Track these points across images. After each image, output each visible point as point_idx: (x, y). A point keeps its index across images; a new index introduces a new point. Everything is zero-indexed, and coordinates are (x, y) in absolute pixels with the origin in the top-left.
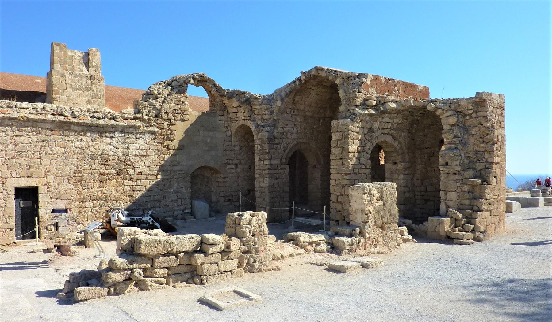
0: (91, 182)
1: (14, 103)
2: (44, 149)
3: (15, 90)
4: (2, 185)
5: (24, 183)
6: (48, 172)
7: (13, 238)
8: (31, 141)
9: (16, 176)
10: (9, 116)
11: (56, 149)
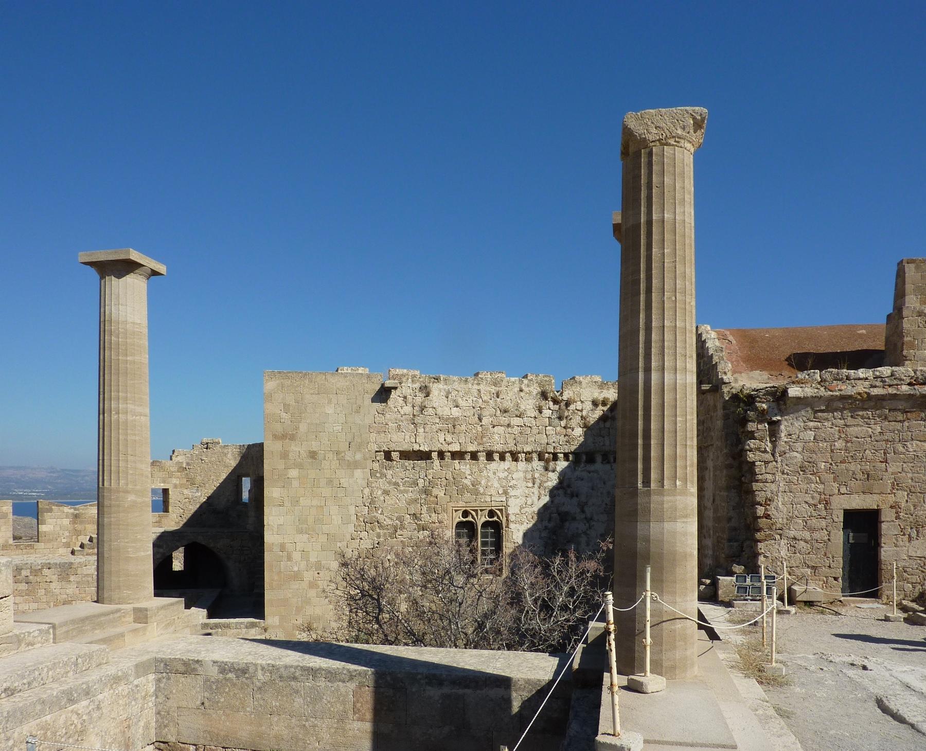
1: (845, 372)
2: (892, 446)
3: (831, 351)
4: (825, 506)
5: (858, 502)
6: (897, 484)
7: (838, 594)
8: (871, 433)
9: (846, 492)
10: (841, 395)
11: (912, 444)
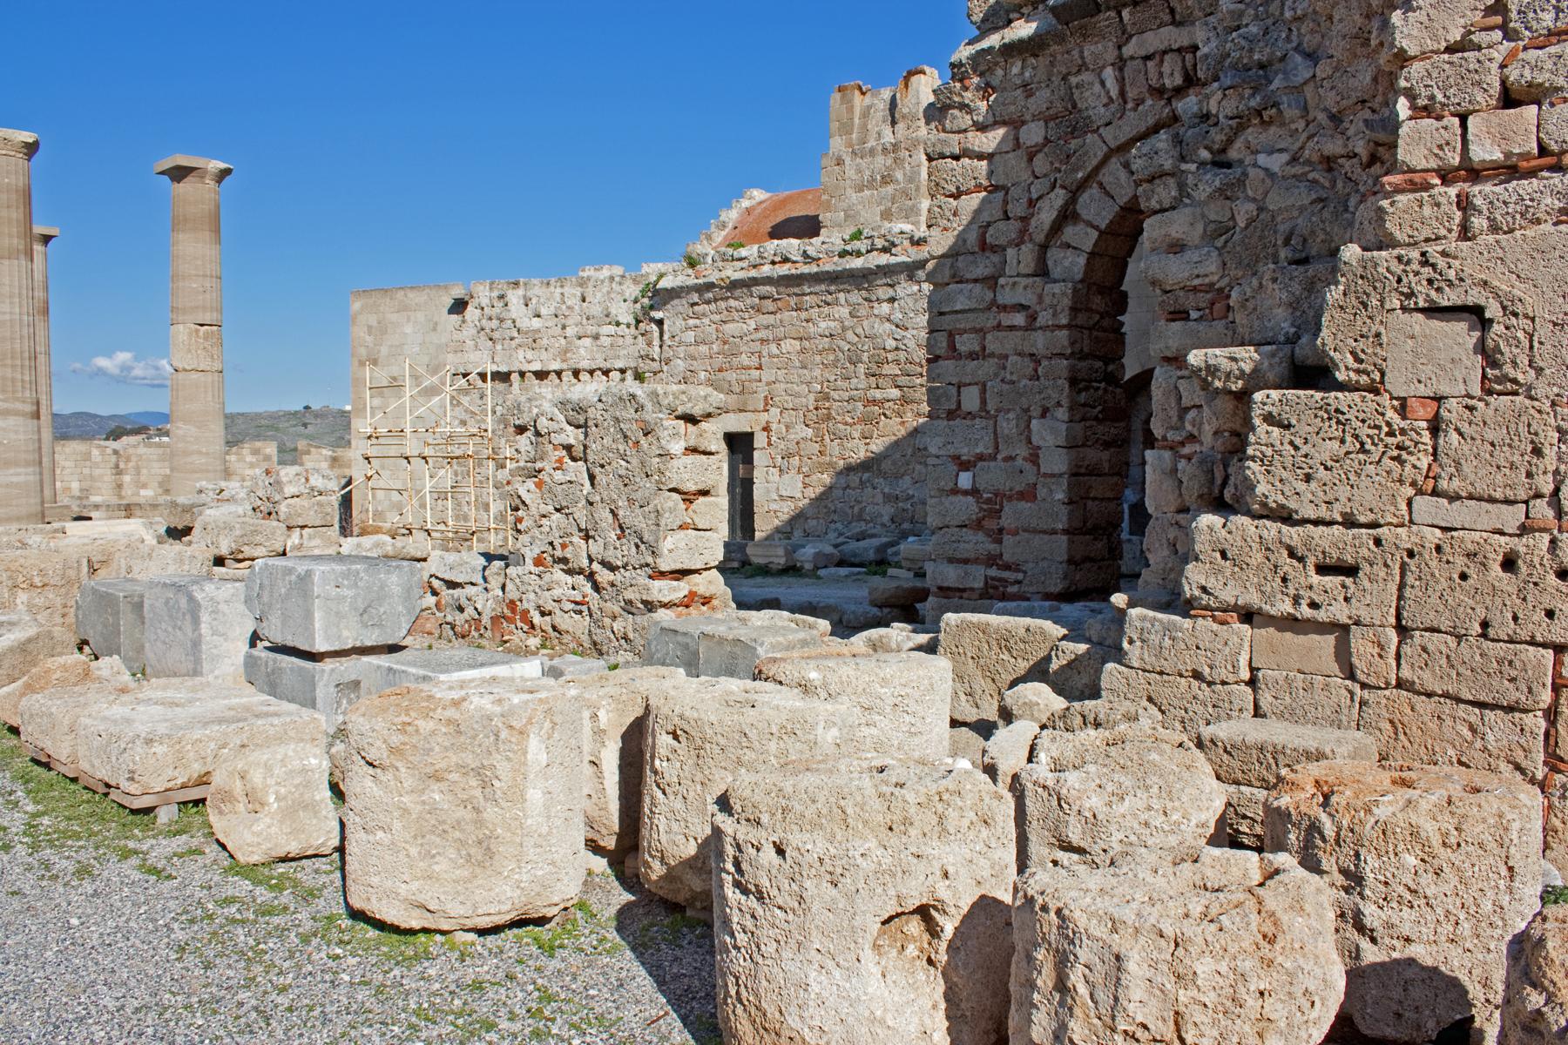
0: (846, 424)
